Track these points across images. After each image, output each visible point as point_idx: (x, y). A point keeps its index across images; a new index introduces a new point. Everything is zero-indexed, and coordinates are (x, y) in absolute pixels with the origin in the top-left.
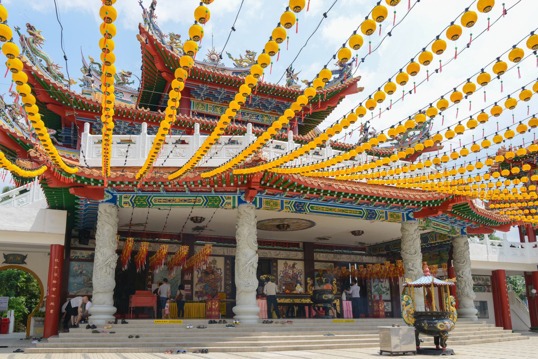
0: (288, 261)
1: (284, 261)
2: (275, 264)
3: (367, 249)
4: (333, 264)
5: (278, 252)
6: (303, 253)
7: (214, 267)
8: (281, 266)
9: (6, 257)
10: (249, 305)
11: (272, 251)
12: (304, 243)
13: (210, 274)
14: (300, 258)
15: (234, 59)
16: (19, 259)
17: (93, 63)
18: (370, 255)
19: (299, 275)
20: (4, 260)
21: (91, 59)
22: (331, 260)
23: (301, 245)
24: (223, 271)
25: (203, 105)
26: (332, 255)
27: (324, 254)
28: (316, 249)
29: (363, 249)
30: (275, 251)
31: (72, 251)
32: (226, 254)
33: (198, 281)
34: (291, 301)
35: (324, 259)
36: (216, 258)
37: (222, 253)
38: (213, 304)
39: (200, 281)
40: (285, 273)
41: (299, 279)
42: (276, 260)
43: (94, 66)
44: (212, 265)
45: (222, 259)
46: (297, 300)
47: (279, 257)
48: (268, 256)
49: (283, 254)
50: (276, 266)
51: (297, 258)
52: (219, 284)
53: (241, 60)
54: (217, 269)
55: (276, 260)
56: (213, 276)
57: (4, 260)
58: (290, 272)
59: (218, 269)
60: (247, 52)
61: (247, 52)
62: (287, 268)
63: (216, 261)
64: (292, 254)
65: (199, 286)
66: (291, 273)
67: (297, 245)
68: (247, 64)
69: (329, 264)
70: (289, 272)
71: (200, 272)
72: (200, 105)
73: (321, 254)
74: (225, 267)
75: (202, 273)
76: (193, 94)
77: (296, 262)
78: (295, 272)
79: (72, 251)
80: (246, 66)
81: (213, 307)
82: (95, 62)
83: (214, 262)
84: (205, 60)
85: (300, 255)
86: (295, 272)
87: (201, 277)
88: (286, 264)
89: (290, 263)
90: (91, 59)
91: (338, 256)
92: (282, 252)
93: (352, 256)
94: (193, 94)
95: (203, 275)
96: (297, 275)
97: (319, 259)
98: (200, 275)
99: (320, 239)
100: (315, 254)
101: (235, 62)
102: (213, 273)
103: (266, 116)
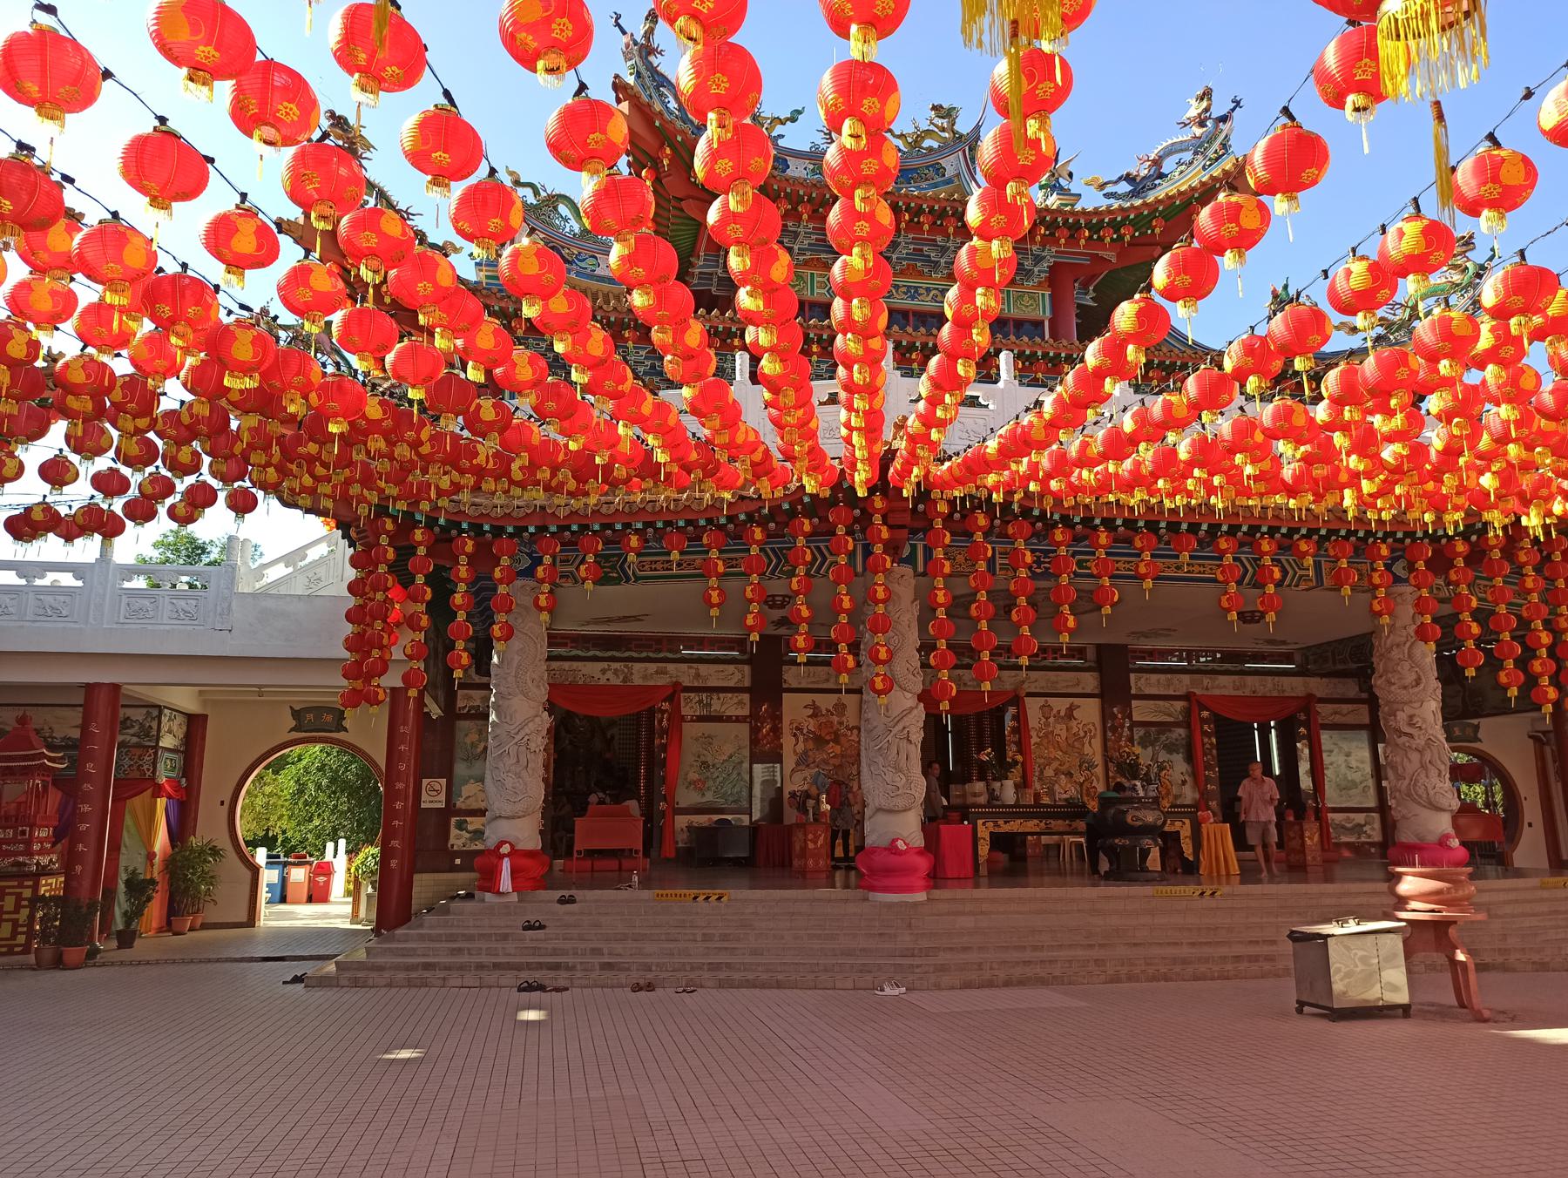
0: (1051, 700)
1: (1041, 700)
3: (1297, 657)
7: (841, 723)
9: (296, 714)
13: (828, 742)
16: (329, 718)
19: (1086, 740)
20: (293, 723)
23: (1091, 654)
26: (1186, 678)
27: (1162, 677)
29: (1288, 658)
33: (798, 764)
38: (810, 836)
40: (1046, 735)
44: (835, 719)
46: (1060, 822)
47: (1028, 688)
54: (848, 728)
56: (838, 749)
57: (293, 723)
58: (1060, 730)
62: (1051, 720)
64: (1064, 680)
65: (798, 777)
66: (1064, 734)
68: (935, 145)
71: (801, 738)
73: (1154, 677)
75: (806, 741)
77: (1077, 701)
80: (930, 149)
81: (811, 845)
83: (840, 708)
84: (815, 145)
85: (1090, 681)
87: (805, 752)
88: (1046, 708)
89: (1060, 705)
91: (1206, 680)
93: (1249, 679)
95: (811, 745)
96: (1080, 739)
97: (1148, 691)
98: (801, 747)
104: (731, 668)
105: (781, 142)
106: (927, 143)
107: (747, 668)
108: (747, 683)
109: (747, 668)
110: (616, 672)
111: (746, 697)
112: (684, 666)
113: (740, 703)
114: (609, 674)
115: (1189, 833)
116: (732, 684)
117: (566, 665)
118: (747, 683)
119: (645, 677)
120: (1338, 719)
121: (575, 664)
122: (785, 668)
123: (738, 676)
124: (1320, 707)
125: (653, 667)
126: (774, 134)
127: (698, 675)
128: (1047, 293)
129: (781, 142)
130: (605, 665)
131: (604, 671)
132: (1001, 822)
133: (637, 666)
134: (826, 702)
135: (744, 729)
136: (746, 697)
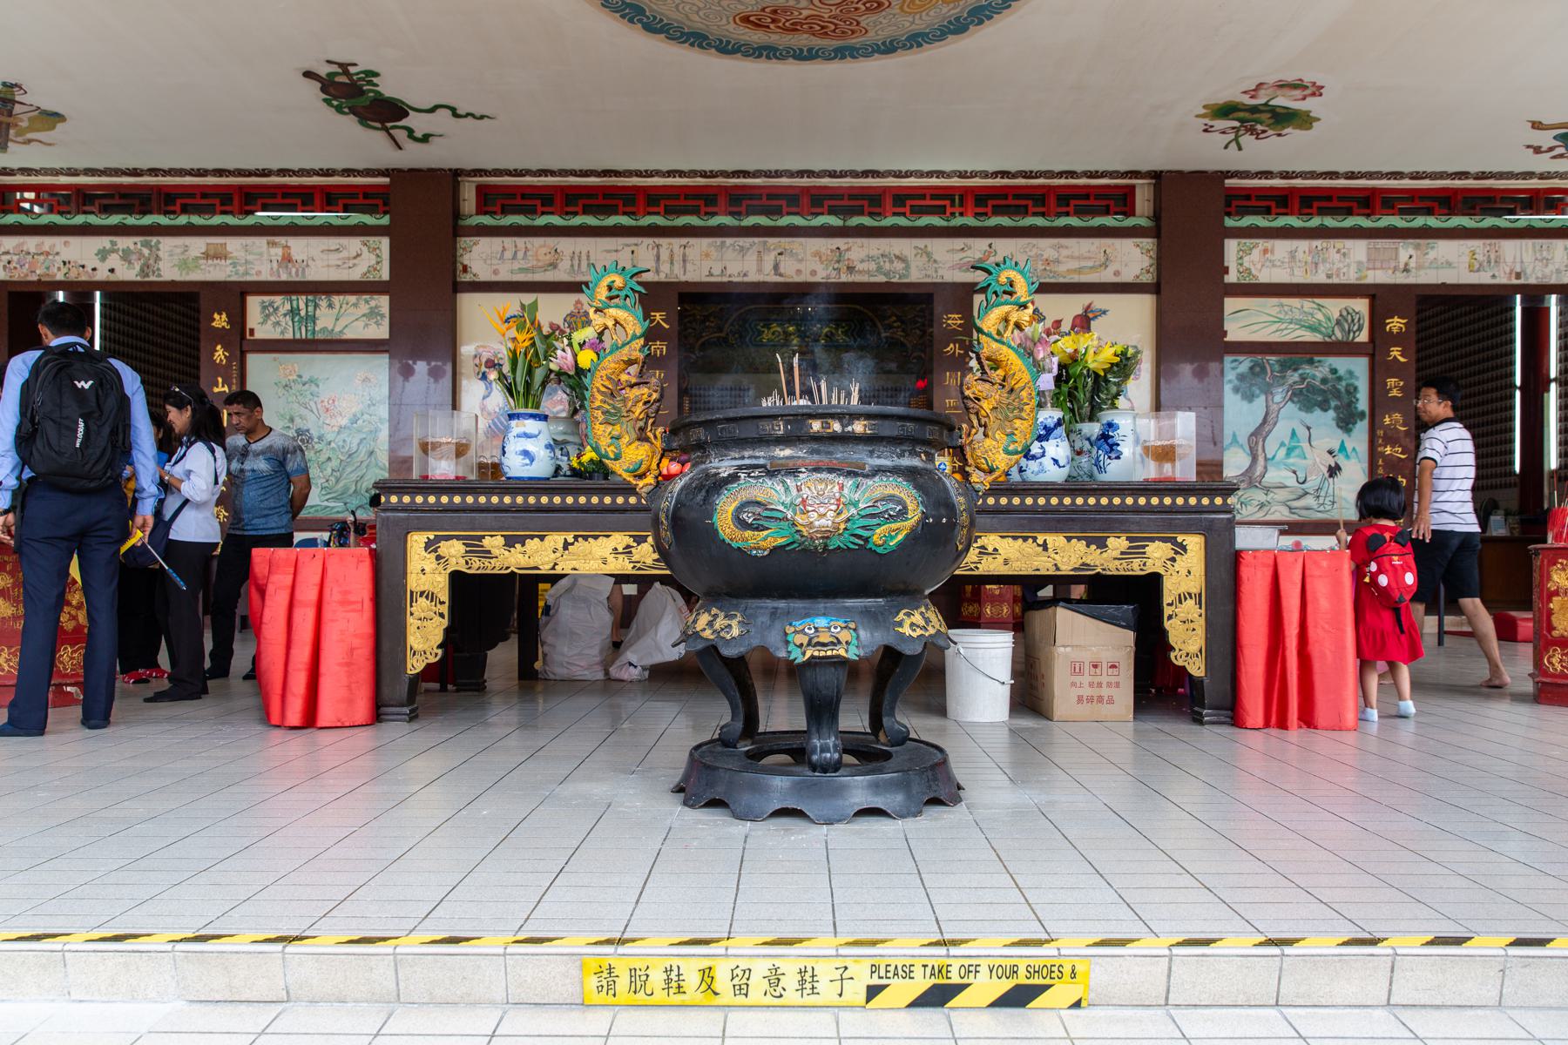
4: (1361, 306)
6: (1148, 243)
11: (939, 246)
14: (1128, 276)
22: (1351, 277)
27: (1303, 245)
28: (1243, 212)
30: (959, 243)
35: (1299, 277)
48: (916, 276)
51: (1107, 276)
69: (1334, 306)
73: (1282, 247)
77: (1099, 301)
97: (1265, 276)
100: (1232, 247)
104: (354, 244)
107: (385, 243)
110: (126, 256)
112: (260, 242)
113: (373, 314)
114: (114, 261)
116: (355, 275)
118: (385, 275)
119: (184, 265)
121: (48, 242)
122: (464, 242)
123: (368, 260)
125: (198, 245)
127: (287, 259)
130: (104, 242)
131: (103, 255)
133: (167, 244)
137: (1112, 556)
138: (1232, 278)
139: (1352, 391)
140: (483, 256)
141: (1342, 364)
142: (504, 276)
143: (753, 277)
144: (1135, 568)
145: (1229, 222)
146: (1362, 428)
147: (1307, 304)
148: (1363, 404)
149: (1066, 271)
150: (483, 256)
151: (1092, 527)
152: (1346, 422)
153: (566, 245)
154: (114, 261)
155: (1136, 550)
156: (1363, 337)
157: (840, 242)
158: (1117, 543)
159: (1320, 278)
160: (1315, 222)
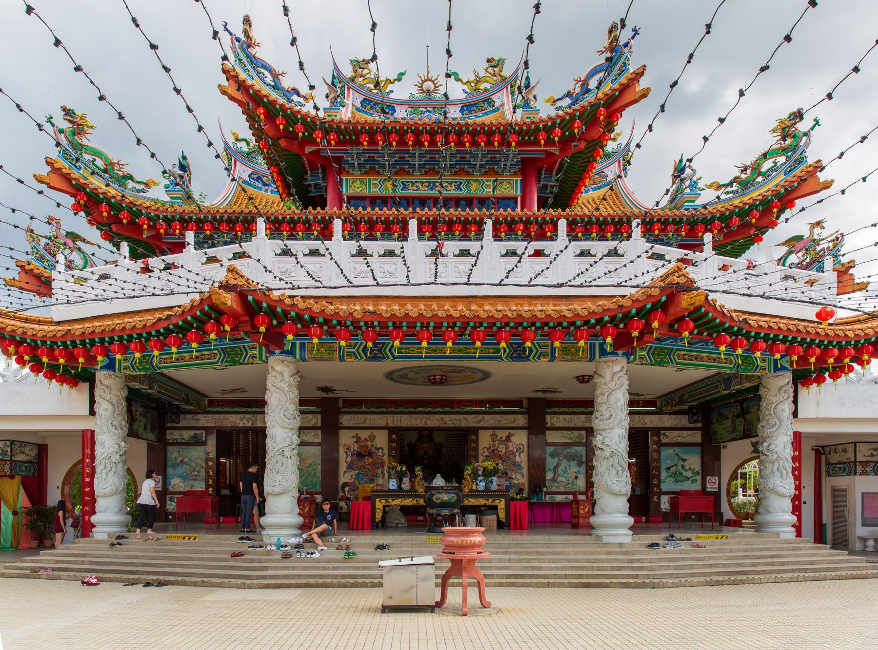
0: (497, 432)
1: (491, 432)
2: (473, 437)
4: (584, 433)
5: (480, 416)
6: (526, 416)
7: (372, 446)
8: (485, 440)
10: (281, 511)
11: (469, 417)
12: (530, 400)
13: (364, 456)
14: (520, 425)
15: (465, 81)
17: (237, 140)
18: (659, 413)
19: (517, 454)
21: (234, 134)
22: (581, 425)
23: (525, 404)
24: (386, 451)
25: (362, 182)
27: (567, 416)
28: (550, 407)
29: (651, 403)
30: (475, 416)
31: (168, 432)
32: (391, 425)
33: (348, 468)
34: (414, 502)
35: (567, 425)
36: (375, 432)
37: (383, 424)
39: (350, 467)
40: (493, 451)
41: (518, 459)
42: (475, 430)
43: (239, 144)
44: (369, 443)
45: (386, 432)
47: (481, 424)
48: (463, 425)
49: (490, 420)
50: (476, 441)
51: (515, 425)
52: (380, 471)
53: (478, 81)
54: (376, 448)
55: (475, 430)
56: (370, 460)
58: (503, 449)
59: (378, 449)
60: (489, 61)
61: (489, 61)
62: (497, 442)
63: (374, 437)
64: (506, 420)
67: (518, 403)
68: (488, 86)
69: (576, 433)
70: (500, 449)
72: (358, 182)
73: (562, 417)
74: (390, 446)
75: (352, 455)
76: (346, 166)
77: (513, 432)
78: (511, 448)
79: (168, 432)
80: (486, 90)
82: (240, 138)
83: (372, 437)
85: (521, 420)
86: (511, 448)
87: (352, 462)
88: (493, 436)
89: (503, 434)
90: (234, 134)
92: (487, 417)
94: (346, 166)
95: (355, 458)
97: (558, 425)
98: (349, 459)
99: (545, 391)
100: (548, 417)
101: (465, 87)
102: (370, 454)
103: (475, 181)
104: (310, 416)
105: (392, 96)
106: (483, 86)
107: (319, 416)
108: (319, 424)
109: (319, 416)
110: (248, 420)
111: (319, 432)
113: (316, 435)
114: (245, 421)
115: (503, 506)
116: (311, 425)
117: (222, 416)
118: (319, 424)
120: (680, 440)
121: (226, 416)
122: (340, 416)
123: (314, 421)
124: (667, 433)
126: (387, 90)
128: (519, 179)
129: (392, 96)
130: (242, 416)
131: (241, 419)
132: (390, 500)
134: (364, 434)
135: (317, 450)
136: (319, 432)
137: (490, 502)
138: (548, 425)
139: (581, 456)
140: (346, 420)
141: (578, 449)
142: (351, 425)
143: (419, 425)
144: (493, 504)
145: (547, 410)
146: (584, 465)
147: (569, 432)
148: (584, 459)
149: (503, 424)
150: (346, 420)
151: (486, 497)
152: (579, 465)
153: (368, 417)
154: (245, 421)
155: (494, 501)
156: (584, 441)
157: (443, 416)
158: (491, 500)
159: (572, 425)
160: (571, 410)
